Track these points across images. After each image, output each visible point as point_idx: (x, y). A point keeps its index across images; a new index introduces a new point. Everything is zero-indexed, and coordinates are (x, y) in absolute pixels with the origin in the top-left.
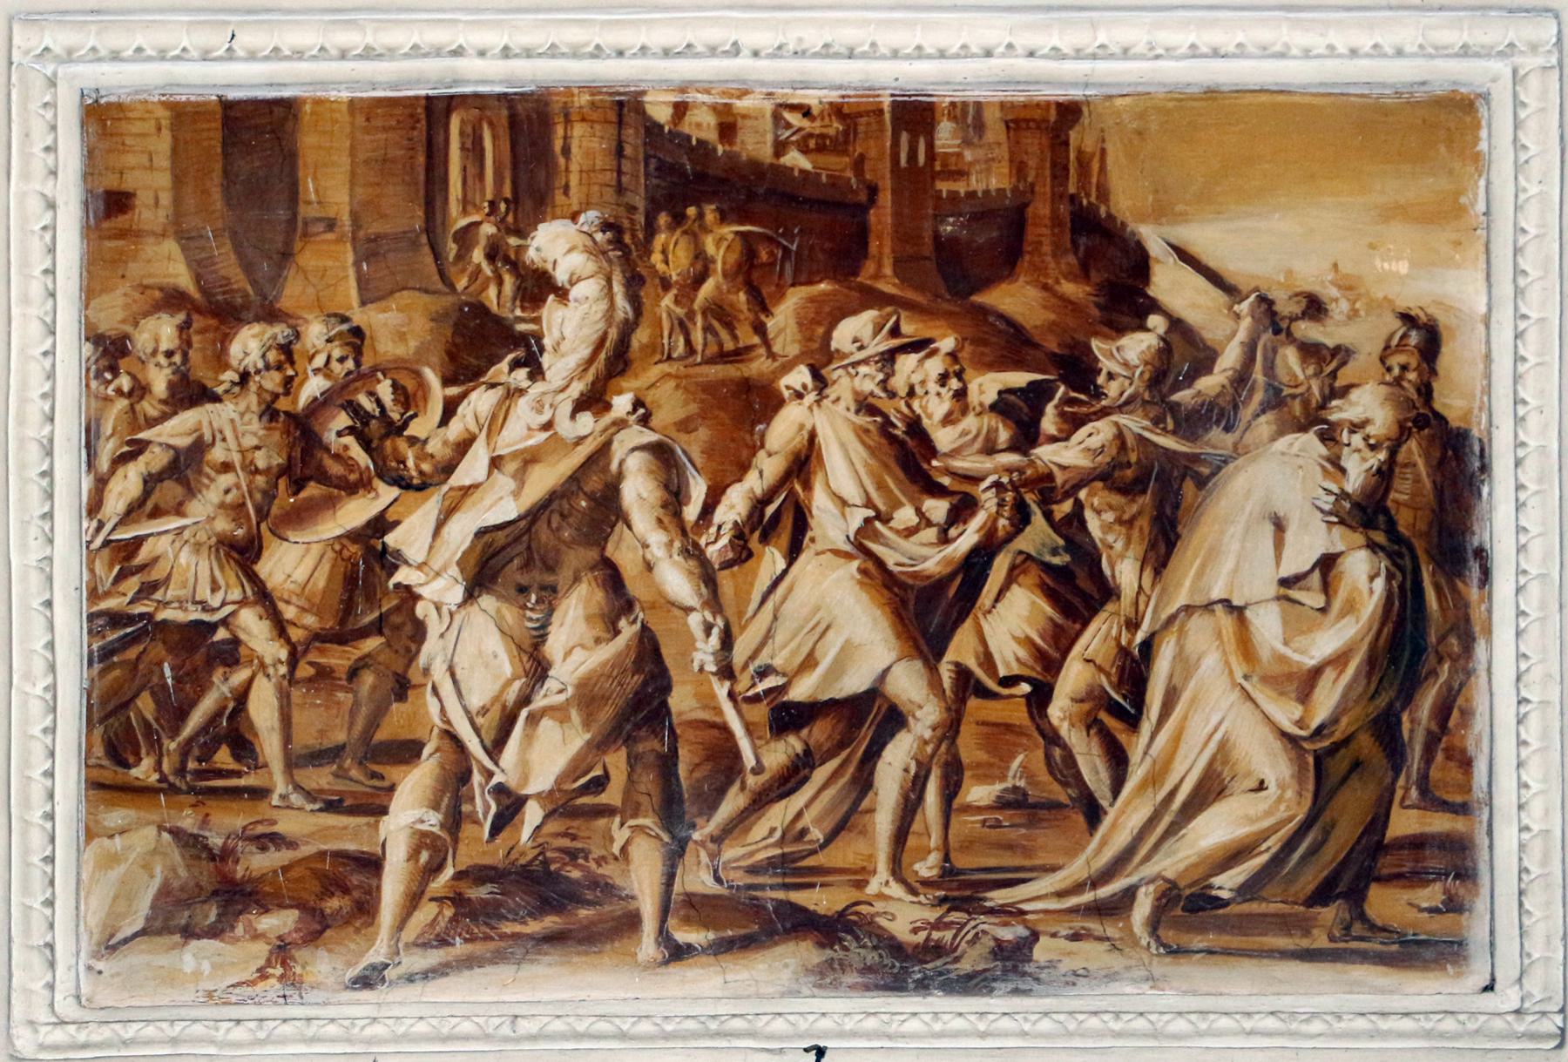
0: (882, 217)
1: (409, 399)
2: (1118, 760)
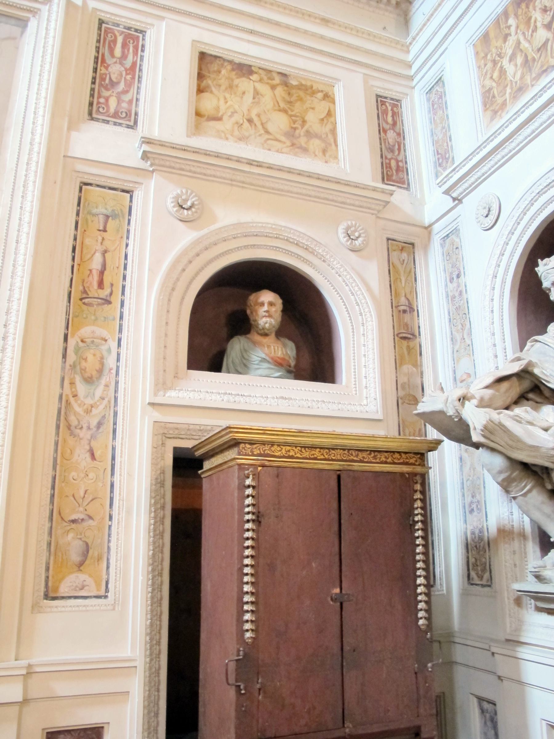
1: (501, 49)
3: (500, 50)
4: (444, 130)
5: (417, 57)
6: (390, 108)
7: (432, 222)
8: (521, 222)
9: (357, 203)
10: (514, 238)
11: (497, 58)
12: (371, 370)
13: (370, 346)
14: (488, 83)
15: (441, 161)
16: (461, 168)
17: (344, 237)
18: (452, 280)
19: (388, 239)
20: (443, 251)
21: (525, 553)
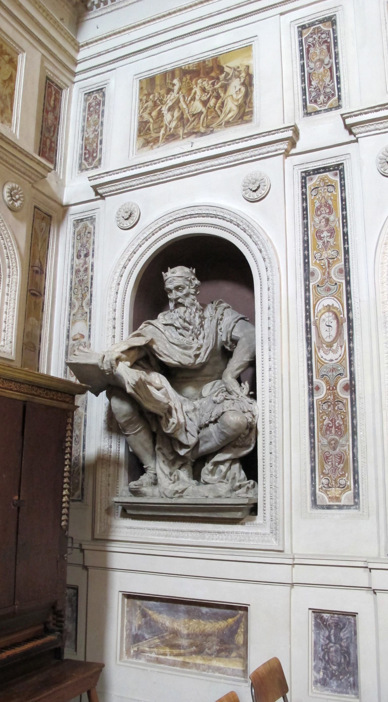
0: (202, 71)
1: (163, 97)
2: (221, 111)
3: (162, 97)
4: (96, 133)
5: (85, 60)
6: (54, 92)
7: (71, 203)
8: (156, 234)
9: (23, 169)
10: (147, 244)
11: (158, 102)
12: (11, 317)
13: (13, 296)
14: (146, 116)
15: (87, 156)
16: (114, 174)
17: (8, 197)
18: (79, 257)
19: (35, 207)
20: (75, 231)
21: (118, 476)
